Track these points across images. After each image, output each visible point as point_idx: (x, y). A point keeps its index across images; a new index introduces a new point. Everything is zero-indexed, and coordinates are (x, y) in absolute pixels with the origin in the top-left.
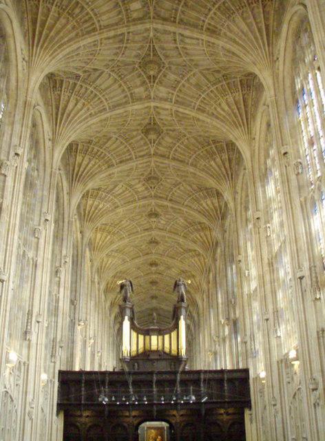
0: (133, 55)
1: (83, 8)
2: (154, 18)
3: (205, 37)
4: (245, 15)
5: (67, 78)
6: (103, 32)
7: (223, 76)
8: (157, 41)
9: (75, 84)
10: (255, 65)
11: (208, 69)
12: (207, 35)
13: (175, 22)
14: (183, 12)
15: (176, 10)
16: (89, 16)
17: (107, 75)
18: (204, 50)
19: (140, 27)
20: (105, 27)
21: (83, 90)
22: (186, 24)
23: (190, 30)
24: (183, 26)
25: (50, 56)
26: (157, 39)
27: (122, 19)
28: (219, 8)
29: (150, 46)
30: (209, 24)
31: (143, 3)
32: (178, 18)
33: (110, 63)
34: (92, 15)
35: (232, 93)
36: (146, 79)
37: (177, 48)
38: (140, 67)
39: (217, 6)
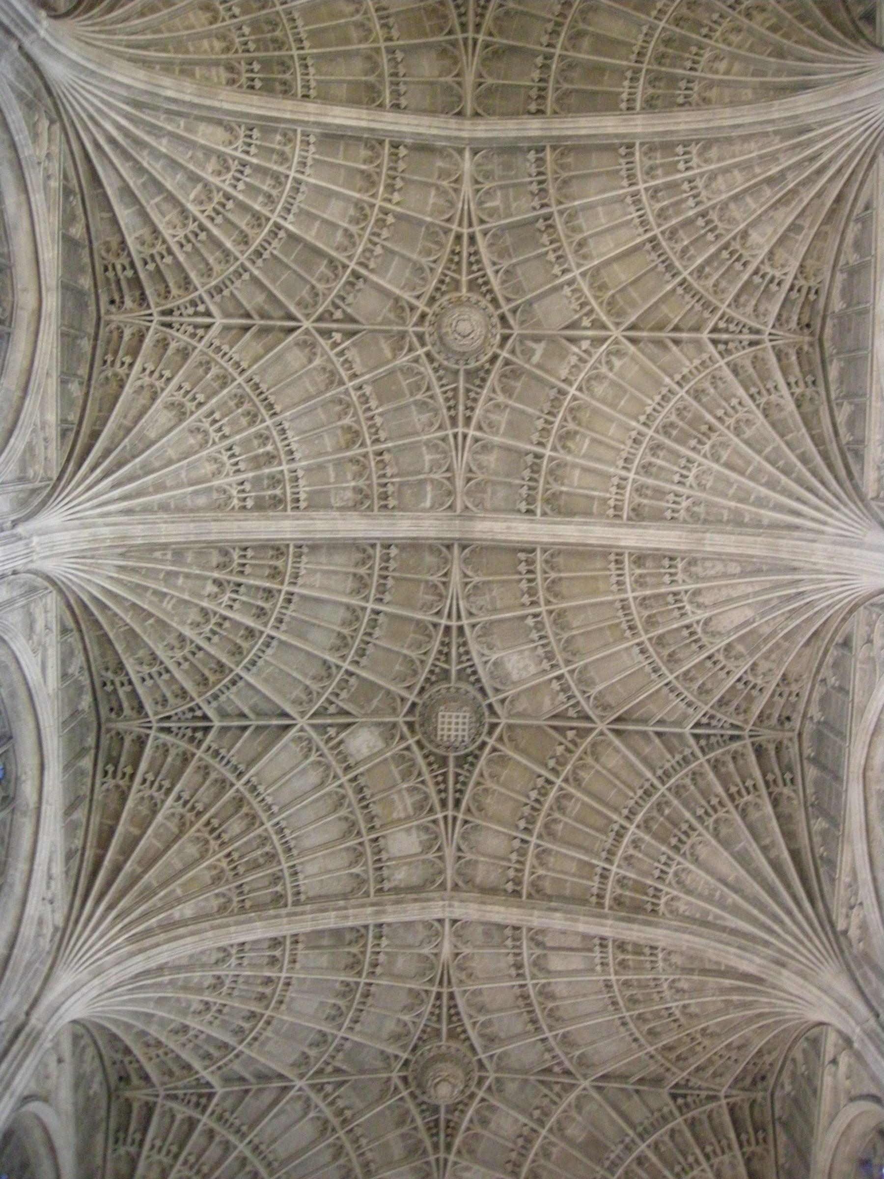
0: (385, 1034)
1: (253, 819)
2: (456, 887)
3: (610, 929)
4: (724, 831)
5: (168, 1097)
6: (303, 913)
7: (674, 1097)
8: (463, 976)
9: (191, 1124)
10: (783, 965)
11: (623, 1077)
12: (622, 919)
13: (517, 893)
14: (542, 854)
15: (522, 853)
16: (267, 849)
17: (299, 1106)
18: (608, 986)
19: (412, 912)
20: (310, 900)
21: (214, 1151)
22: (550, 898)
23: (566, 912)
24: (545, 904)
25: (131, 940)
26: (461, 968)
27: (361, 881)
28: (646, 825)
29: (439, 996)
30: (621, 881)
31: (425, 837)
32: (526, 878)
33: (313, 1053)
34: (280, 849)
35: (707, 1157)
36: (423, 1135)
37: (525, 997)
38: (405, 1079)
39: (639, 818)
